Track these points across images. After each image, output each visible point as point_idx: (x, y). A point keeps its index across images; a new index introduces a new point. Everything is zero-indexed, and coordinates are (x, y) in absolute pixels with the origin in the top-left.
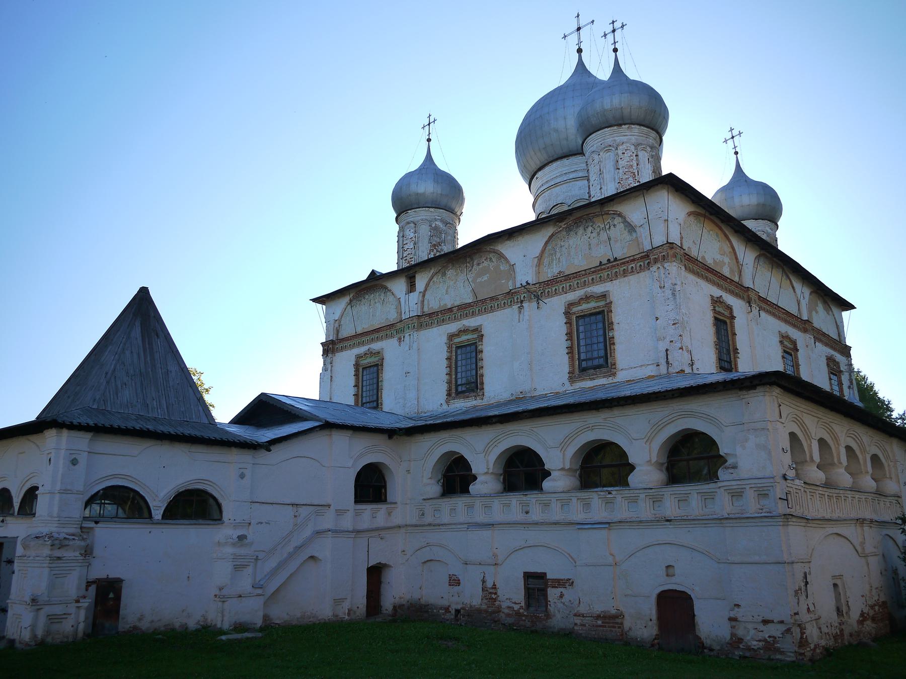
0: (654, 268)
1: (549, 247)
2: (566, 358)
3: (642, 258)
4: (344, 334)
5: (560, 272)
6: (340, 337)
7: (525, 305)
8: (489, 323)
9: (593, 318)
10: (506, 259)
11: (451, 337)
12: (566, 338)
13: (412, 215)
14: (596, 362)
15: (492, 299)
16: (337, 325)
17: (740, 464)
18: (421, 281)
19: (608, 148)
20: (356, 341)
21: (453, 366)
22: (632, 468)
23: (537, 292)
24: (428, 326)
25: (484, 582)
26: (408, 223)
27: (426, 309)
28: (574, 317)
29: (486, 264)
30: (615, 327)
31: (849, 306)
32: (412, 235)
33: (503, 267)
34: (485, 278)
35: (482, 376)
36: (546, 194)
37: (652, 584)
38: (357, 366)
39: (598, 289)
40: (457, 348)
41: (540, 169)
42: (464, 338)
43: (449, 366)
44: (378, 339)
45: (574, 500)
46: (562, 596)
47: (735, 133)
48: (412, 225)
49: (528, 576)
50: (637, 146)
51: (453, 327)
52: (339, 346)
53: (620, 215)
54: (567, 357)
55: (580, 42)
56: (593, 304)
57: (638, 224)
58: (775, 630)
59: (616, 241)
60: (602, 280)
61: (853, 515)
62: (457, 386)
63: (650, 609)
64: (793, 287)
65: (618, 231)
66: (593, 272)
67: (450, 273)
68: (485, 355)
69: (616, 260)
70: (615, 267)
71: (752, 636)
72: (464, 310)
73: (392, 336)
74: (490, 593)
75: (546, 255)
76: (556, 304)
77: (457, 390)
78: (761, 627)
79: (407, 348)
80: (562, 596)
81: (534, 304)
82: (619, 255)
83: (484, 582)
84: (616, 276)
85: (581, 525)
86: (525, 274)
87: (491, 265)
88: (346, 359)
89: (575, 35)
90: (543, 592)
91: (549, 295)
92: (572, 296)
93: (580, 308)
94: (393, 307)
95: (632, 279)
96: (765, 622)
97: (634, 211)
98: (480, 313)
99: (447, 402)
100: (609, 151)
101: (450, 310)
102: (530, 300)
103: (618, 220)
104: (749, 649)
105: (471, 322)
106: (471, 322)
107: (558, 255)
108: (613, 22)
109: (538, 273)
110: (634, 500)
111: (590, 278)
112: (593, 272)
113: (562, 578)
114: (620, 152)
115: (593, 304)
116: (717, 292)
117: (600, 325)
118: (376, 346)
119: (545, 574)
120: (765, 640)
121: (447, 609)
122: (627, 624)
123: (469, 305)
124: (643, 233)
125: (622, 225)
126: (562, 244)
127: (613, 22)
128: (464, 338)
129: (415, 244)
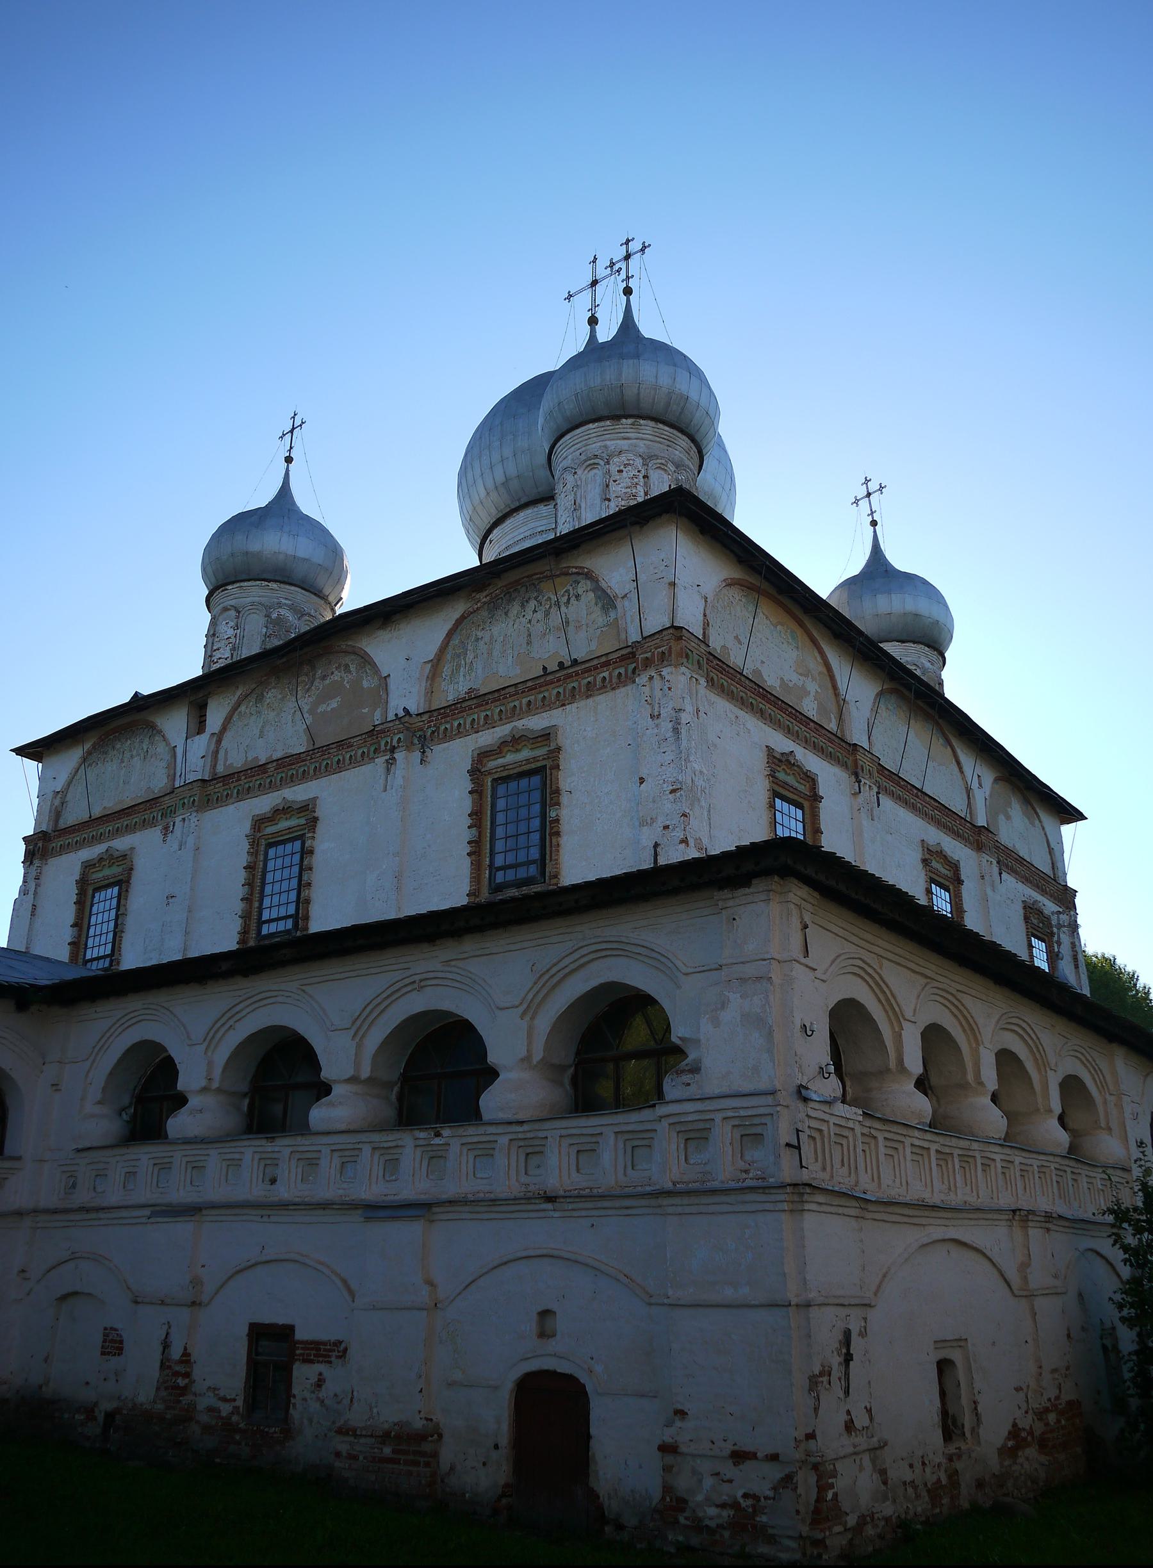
0: (642, 679)
1: (455, 641)
2: (467, 862)
3: (623, 658)
4: (71, 817)
5: (471, 690)
6: (62, 824)
7: (399, 756)
8: (328, 792)
9: (524, 782)
10: (373, 665)
12: (469, 822)
13: (234, 595)
14: (522, 873)
15: (341, 744)
16: (57, 802)
17: (707, 1063)
18: (215, 716)
19: (591, 463)
21: (258, 882)
22: (492, 1074)
24: (221, 801)
25: (166, 1345)
26: (226, 609)
27: (220, 769)
28: (489, 781)
30: (564, 799)
31: (1072, 814)
32: (230, 632)
34: (334, 704)
37: (502, 1355)
39: (536, 723)
42: (284, 824)
43: (249, 883)
45: (367, 1150)
46: (320, 1383)
47: (873, 486)
48: (233, 613)
49: (259, 1333)
50: (647, 459)
51: (263, 804)
52: (56, 844)
53: (589, 575)
54: (468, 861)
55: (595, 306)
56: (525, 754)
57: (620, 593)
58: (757, 1479)
59: (578, 628)
60: (546, 705)
61: (1006, 1200)
63: (495, 1416)
64: (958, 763)
65: (582, 606)
66: (531, 689)
67: (272, 695)
69: (575, 662)
70: (573, 680)
71: (709, 1492)
72: (289, 768)
73: (152, 823)
74: (177, 1371)
76: (455, 756)
78: (729, 1470)
79: (176, 846)
80: (320, 1383)
82: (580, 654)
83: (166, 1345)
84: (573, 696)
85: (374, 1210)
86: (406, 696)
87: (347, 678)
88: (66, 869)
89: (588, 294)
90: (285, 1371)
91: (447, 737)
92: (487, 738)
93: (501, 761)
94: (164, 764)
95: (602, 701)
96: (739, 1457)
97: (614, 568)
98: (317, 774)
100: (593, 466)
101: (262, 768)
102: (409, 748)
103: (584, 586)
104: (698, 1526)
105: (297, 793)
106: (297, 793)
107: (470, 655)
108: (628, 242)
109: (430, 692)
110: (486, 1152)
111: (525, 701)
112: (531, 689)
113: (324, 1337)
114: (614, 469)
115: (525, 754)
116: (783, 744)
117: (536, 796)
118: (121, 844)
119: (291, 1328)
120: (735, 1505)
121: (89, 1411)
122: (447, 1454)
123: (296, 758)
124: (628, 608)
125: (591, 595)
126: (480, 634)
127: (628, 242)
128: (284, 824)
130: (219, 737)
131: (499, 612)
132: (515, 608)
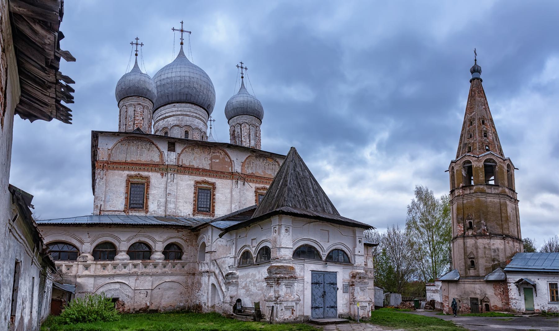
1: (248, 160)
5: (252, 173)
11: (197, 182)
15: (222, 172)
23: (245, 178)
27: (180, 163)
33: (227, 159)
35: (214, 206)
36: (180, 117)
40: (200, 189)
41: (178, 103)
42: (203, 185)
44: (144, 170)
51: (199, 179)
62: (198, 207)
73: (155, 171)
76: (254, 186)
77: (198, 209)
86: (238, 168)
98: (214, 177)
99: (194, 215)
101: (198, 169)
109: (242, 169)
128: (203, 185)
132: (261, 160)
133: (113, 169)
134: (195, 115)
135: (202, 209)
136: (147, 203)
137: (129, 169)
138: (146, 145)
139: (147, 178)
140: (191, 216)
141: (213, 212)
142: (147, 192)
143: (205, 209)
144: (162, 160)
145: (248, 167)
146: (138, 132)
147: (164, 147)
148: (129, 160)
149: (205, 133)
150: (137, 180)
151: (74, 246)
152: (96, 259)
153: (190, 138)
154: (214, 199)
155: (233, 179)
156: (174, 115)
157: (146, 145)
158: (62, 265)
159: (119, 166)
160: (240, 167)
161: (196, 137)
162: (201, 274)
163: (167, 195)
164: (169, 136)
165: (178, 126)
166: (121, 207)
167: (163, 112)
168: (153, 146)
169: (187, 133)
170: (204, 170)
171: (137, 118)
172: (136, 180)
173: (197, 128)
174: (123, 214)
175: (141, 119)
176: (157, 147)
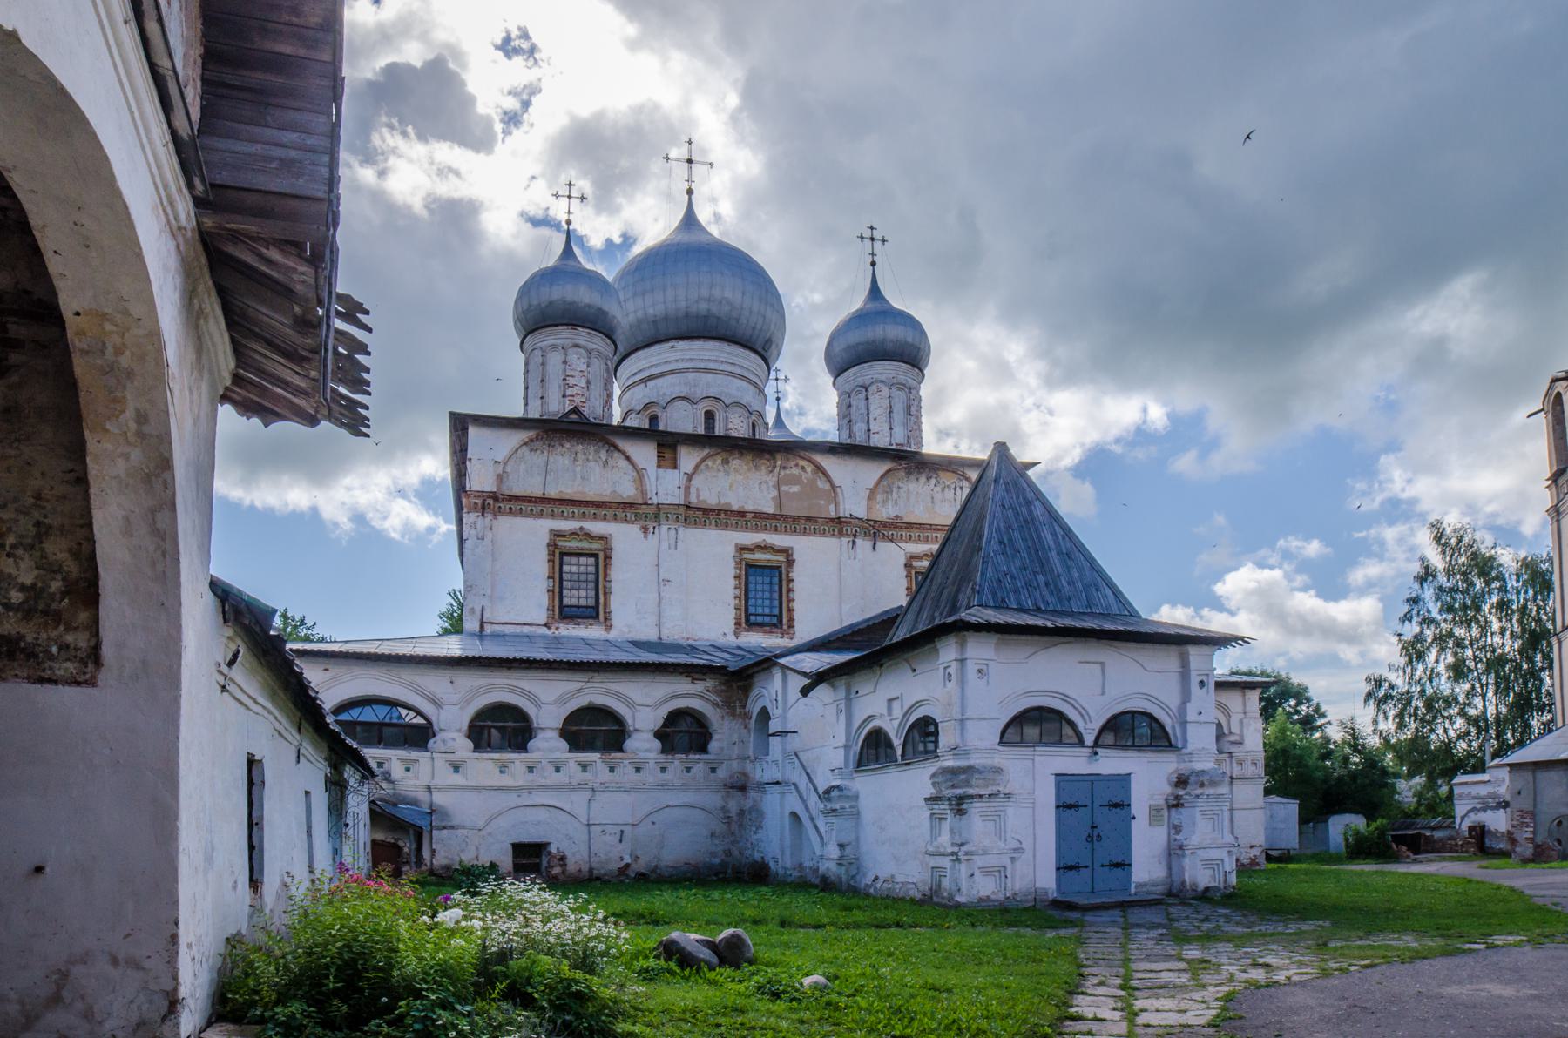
7: (859, 541)
11: (742, 549)
15: (808, 519)
18: (688, 458)
20: (547, 508)
23: (877, 530)
27: (693, 500)
29: (795, 471)
33: (822, 484)
34: (795, 489)
36: (691, 376)
38: (552, 547)
40: (749, 566)
41: (682, 338)
42: (759, 556)
44: (595, 517)
51: (749, 538)
62: (747, 615)
67: (735, 463)
68: (795, 585)
72: (761, 520)
73: (626, 520)
75: (880, 489)
77: (747, 620)
81: (869, 544)
86: (854, 505)
99: (737, 635)
101: (742, 514)
107: (895, 496)
109: (869, 508)
118: (596, 527)
123: (774, 517)
129: (588, 382)
130: (690, 477)
131: (912, 477)
132: (923, 479)
133: (511, 512)
134: (730, 368)
135: (760, 619)
136: (606, 604)
137: (553, 515)
138: (597, 452)
139: (603, 538)
140: (731, 639)
141: (791, 626)
142: (606, 575)
143: (767, 619)
144: (644, 492)
145: (885, 502)
146: (574, 417)
147: (644, 454)
148: (552, 493)
149: (761, 415)
150: (580, 545)
151: (419, 713)
152: (478, 747)
153: (719, 430)
154: (790, 590)
155: (841, 533)
156: (672, 372)
157: (597, 452)
158: (391, 760)
159: (526, 507)
160: (864, 503)
161: (737, 426)
162: (762, 786)
163: (662, 582)
164: (661, 428)
165: (684, 398)
166: (542, 617)
167: (643, 364)
168: (616, 454)
169: (709, 416)
170: (759, 515)
171: (572, 381)
172: (573, 544)
173: (738, 404)
174: (544, 630)
175: (583, 384)
176: (628, 458)
